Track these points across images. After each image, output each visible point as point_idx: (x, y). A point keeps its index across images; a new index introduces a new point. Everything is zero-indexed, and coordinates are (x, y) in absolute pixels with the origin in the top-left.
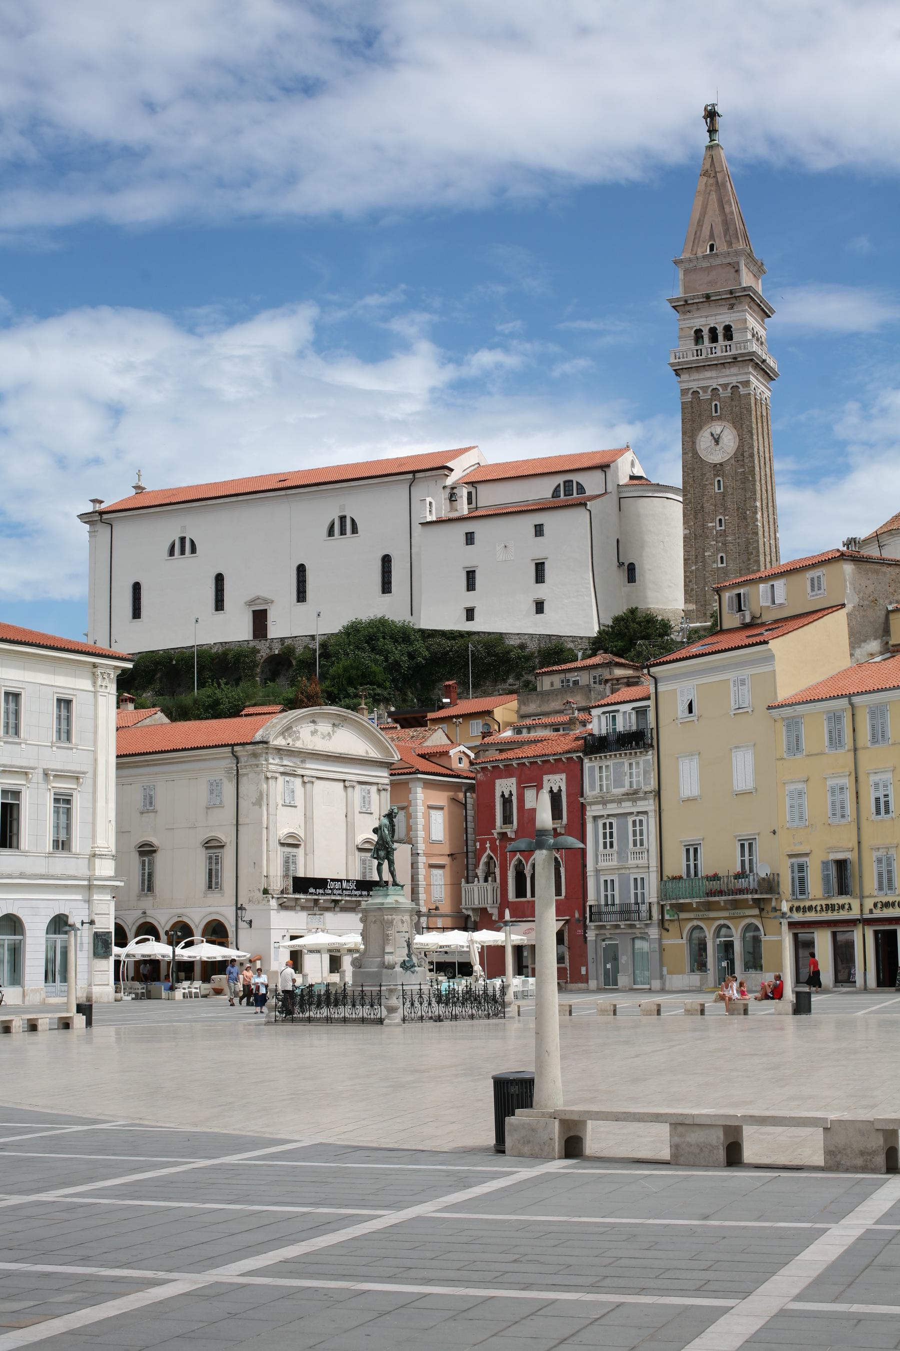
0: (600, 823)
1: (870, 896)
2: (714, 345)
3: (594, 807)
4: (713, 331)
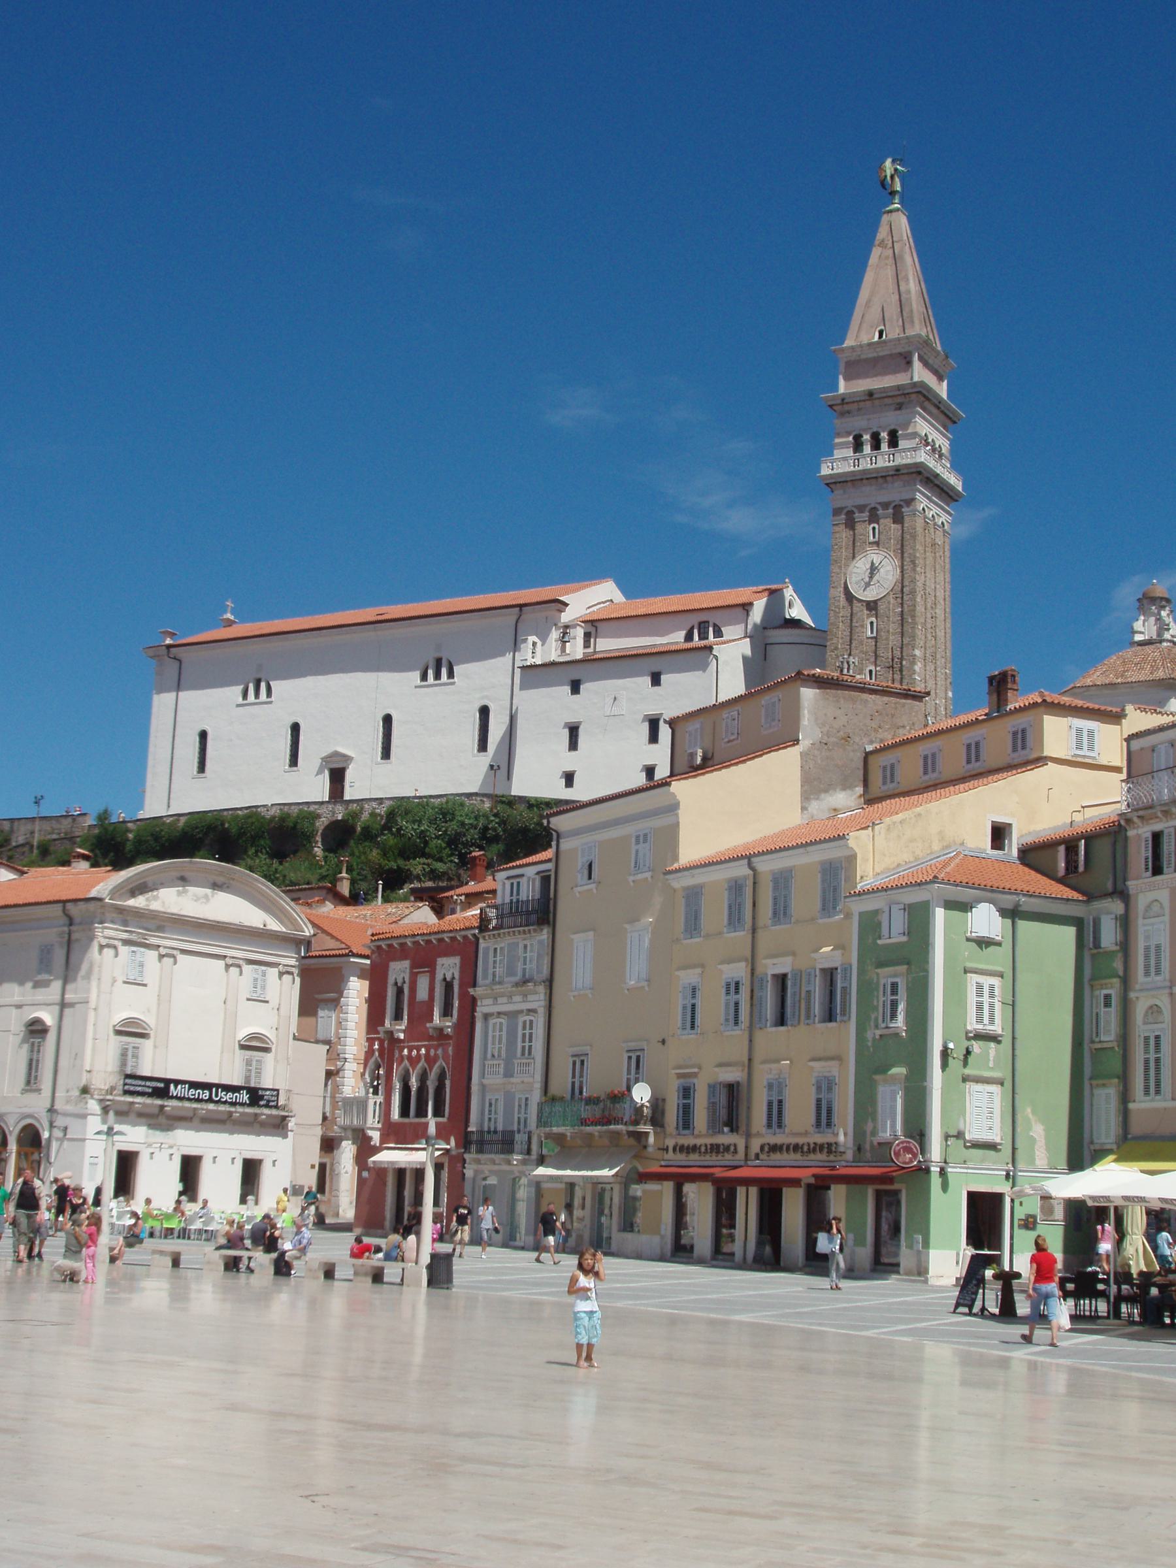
0: (492, 1021)
1: (758, 1134)
3: (486, 1002)
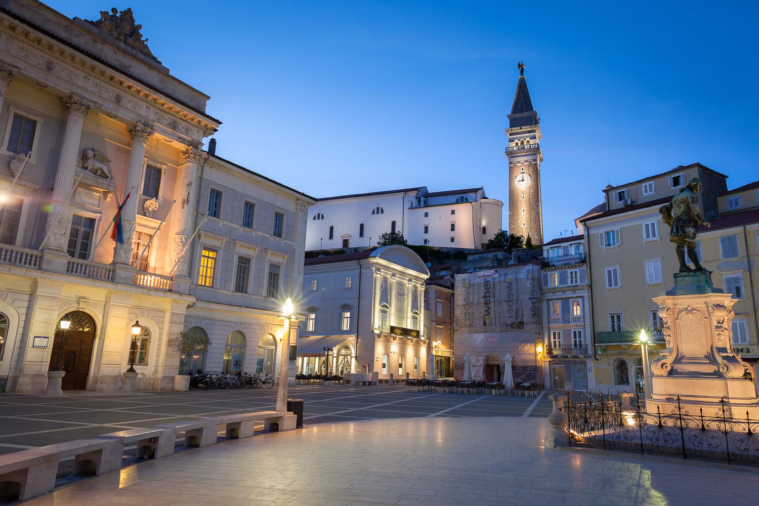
0: (551, 303)
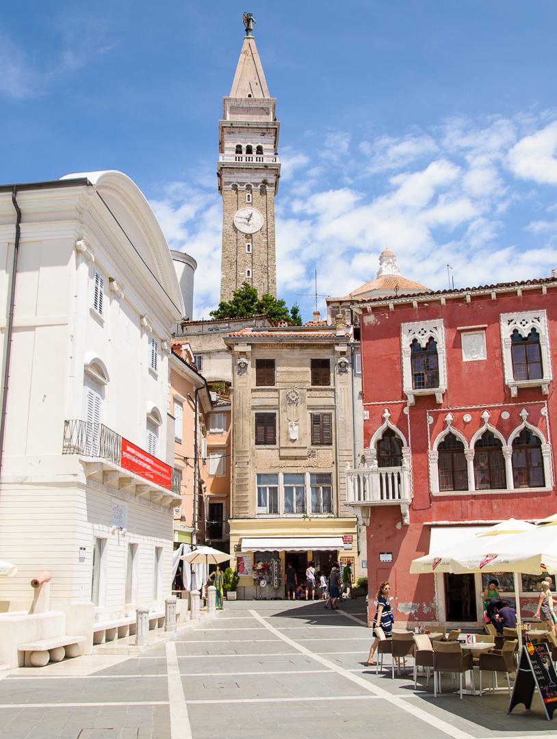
2: (249, 155)
4: (249, 150)
